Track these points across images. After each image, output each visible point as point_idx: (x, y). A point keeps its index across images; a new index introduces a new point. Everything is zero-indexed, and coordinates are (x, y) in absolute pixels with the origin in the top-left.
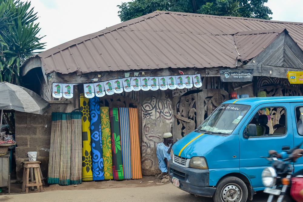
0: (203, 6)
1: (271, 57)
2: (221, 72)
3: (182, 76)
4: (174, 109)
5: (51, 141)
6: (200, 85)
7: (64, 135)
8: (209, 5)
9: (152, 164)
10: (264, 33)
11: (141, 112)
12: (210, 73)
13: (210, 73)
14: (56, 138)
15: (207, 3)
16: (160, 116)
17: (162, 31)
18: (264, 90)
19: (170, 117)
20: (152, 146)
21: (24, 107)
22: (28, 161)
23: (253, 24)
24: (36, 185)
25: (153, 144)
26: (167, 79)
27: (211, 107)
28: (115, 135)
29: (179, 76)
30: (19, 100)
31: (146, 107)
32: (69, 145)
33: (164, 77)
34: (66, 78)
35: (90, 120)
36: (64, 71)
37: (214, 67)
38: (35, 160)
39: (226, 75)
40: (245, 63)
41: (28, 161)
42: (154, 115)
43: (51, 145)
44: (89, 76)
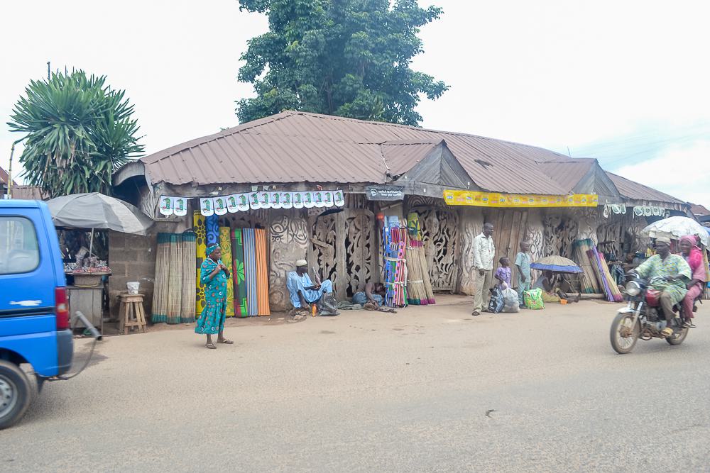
0: (341, 108)
1: (426, 172)
2: (367, 188)
3: (320, 192)
4: (309, 232)
5: (157, 269)
6: (341, 204)
7: (174, 261)
8: (348, 106)
9: (282, 297)
12: (354, 189)
13: (354, 189)
14: (163, 266)
15: (346, 104)
16: (292, 240)
17: (295, 136)
18: (416, 212)
19: (304, 242)
20: (283, 276)
21: (123, 226)
22: (127, 293)
23: (400, 131)
24: (136, 324)
25: (284, 273)
26: (303, 195)
27: (353, 229)
28: (237, 261)
29: (317, 192)
30: (116, 217)
31: (275, 228)
32: (180, 274)
33: (299, 193)
34: (178, 190)
35: (206, 242)
36: (175, 182)
37: (359, 183)
38: (136, 292)
39: (372, 192)
40: (396, 178)
41: (127, 293)
42: (286, 238)
43: (157, 274)
44: (207, 189)
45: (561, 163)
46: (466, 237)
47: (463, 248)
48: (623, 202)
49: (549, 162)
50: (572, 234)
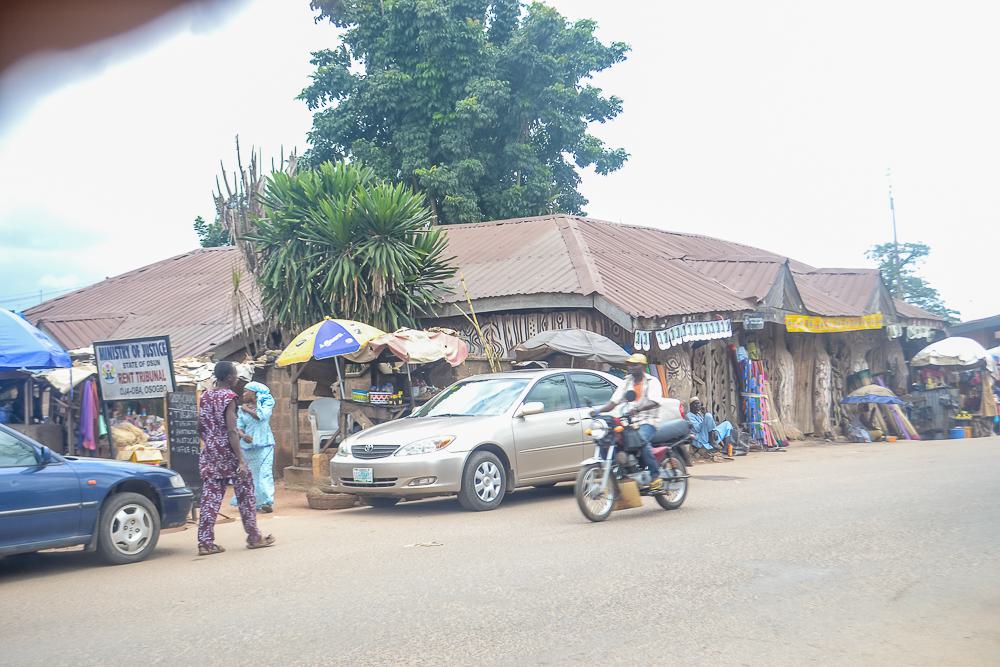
46: (781, 370)
47: (779, 384)
48: (900, 322)
49: (813, 273)
50: (846, 365)
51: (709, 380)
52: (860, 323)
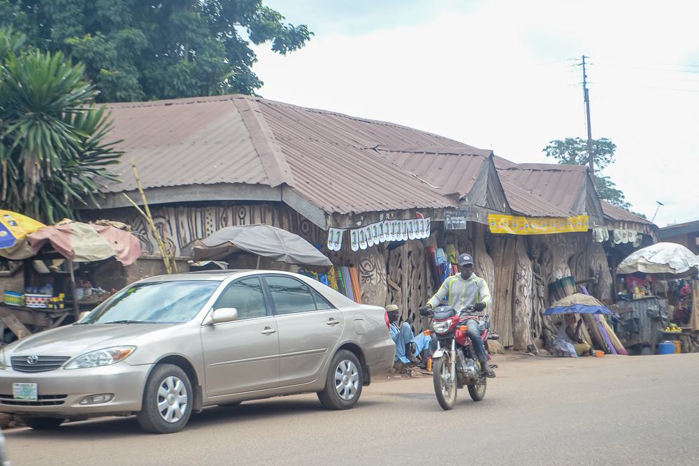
10: (451, 154)
11: (359, 274)
31: (365, 265)
45: (534, 170)
48: (606, 225)
49: (514, 169)
50: (548, 271)
51: (405, 285)
52: (566, 225)
